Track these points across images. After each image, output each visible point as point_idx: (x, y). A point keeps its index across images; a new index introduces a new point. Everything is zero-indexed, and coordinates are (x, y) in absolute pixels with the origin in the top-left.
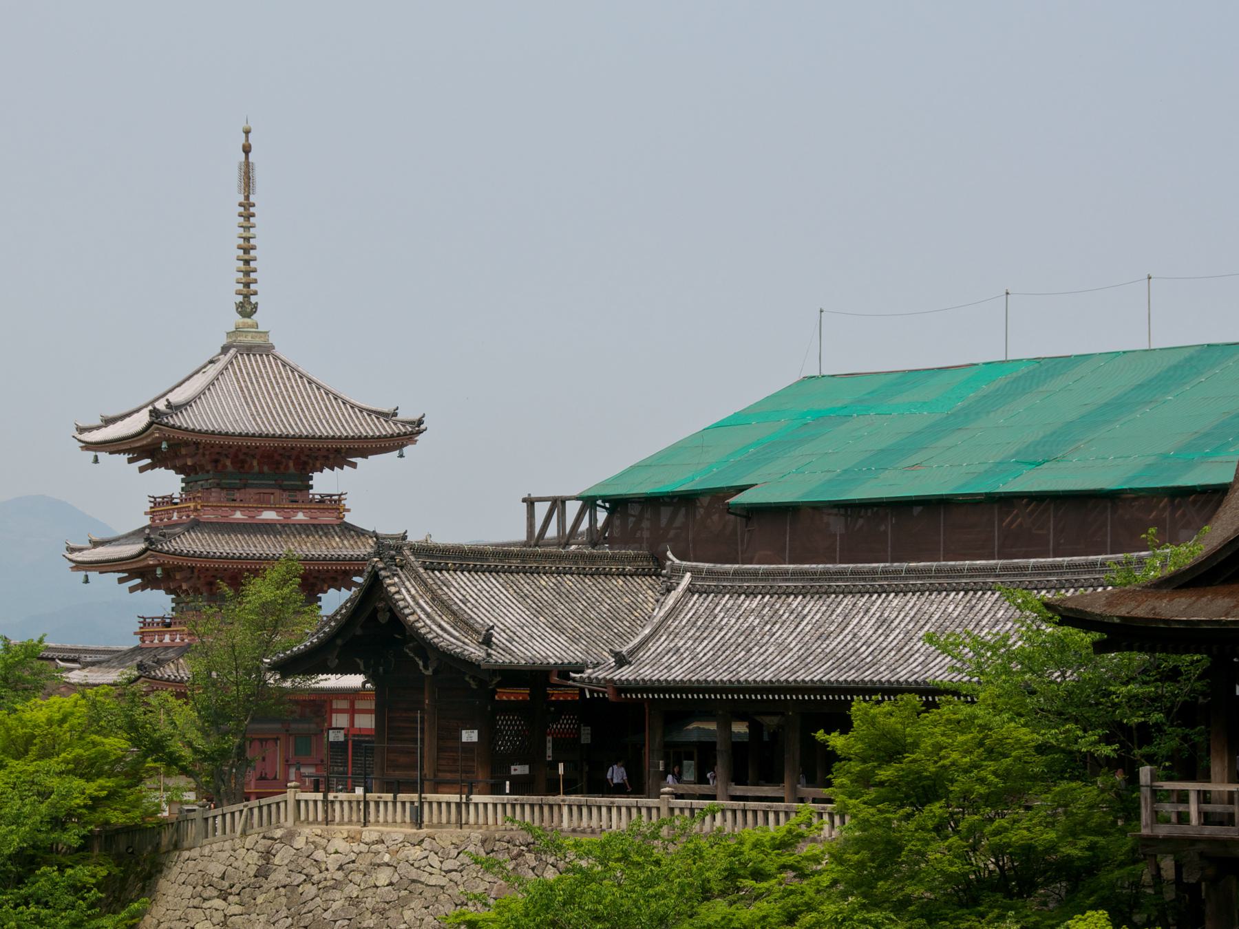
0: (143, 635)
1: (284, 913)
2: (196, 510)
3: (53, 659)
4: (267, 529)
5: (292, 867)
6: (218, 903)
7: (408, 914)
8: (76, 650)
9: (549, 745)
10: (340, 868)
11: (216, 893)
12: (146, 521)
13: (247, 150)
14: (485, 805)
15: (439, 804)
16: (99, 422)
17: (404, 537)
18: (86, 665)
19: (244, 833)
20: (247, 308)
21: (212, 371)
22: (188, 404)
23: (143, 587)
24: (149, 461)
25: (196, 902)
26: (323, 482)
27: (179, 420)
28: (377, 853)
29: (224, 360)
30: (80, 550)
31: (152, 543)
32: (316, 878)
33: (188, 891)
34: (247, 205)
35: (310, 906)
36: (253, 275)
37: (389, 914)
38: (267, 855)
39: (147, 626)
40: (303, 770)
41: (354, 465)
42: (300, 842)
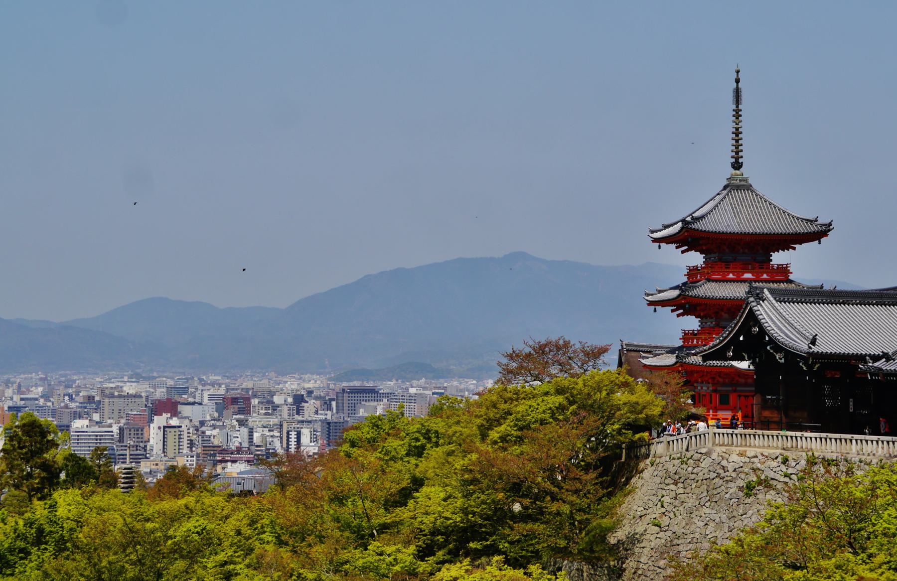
1: (705, 494)
2: (708, 273)
5: (711, 468)
6: (672, 487)
8: (650, 347)
9: (851, 403)
16: (661, 228)
17: (822, 287)
18: (656, 355)
20: (737, 165)
21: (718, 198)
25: (663, 486)
26: (778, 258)
27: (698, 226)
29: (725, 192)
30: (652, 295)
31: (683, 291)
33: (658, 480)
36: (740, 148)
37: (758, 496)
39: (688, 336)
41: (794, 249)
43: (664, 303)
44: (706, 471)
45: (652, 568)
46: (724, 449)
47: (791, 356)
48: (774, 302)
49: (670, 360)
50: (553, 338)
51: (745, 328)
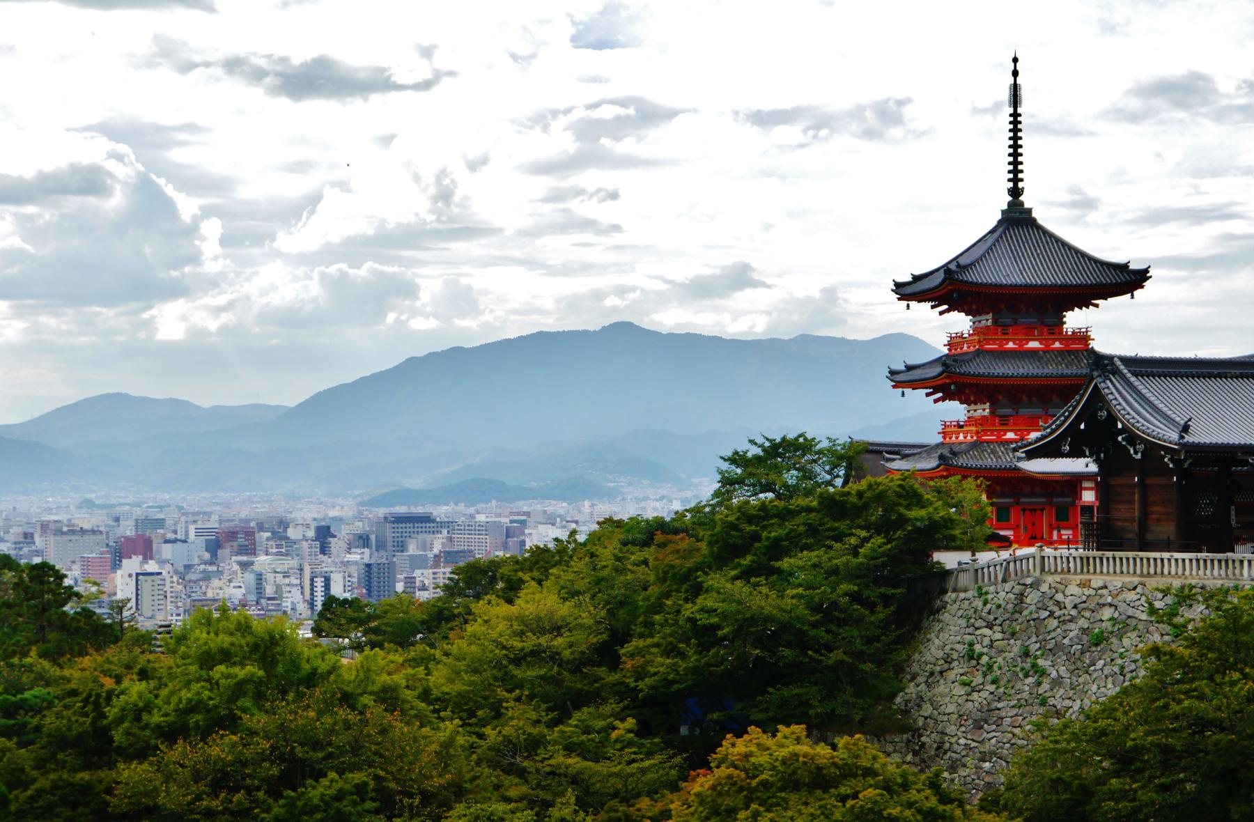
0: (945, 434)
3: (880, 452)
4: (1034, 352)
5: (1040, 605)
6: (986, 631)
7: (1126, 642)
9: (1233, 512)
10: (1075, 607)
11: (985, 624)
12: (945, 350)
13: (1015, 73)
14: (1184, 560)
15: (1148, 559)
16: (909, 279)
18: (905, 457)
19: (1004, 581)
22: (972, 264)
23: (943, 399)
24: (945, 307)
25: (971, 630)
26: (1074, 319)
28: (1101, 596)
32: (1057, 614)
34: (1015, 115)
35: (1053, 635)
38: (1021, 597)
39: (947, 429)
40: (1063, 532)
41: (1097, 306)
42: (1044, 588)
43: (915, 384)
44: (1033, 608)
45: (962, 741)
46: (1058, 578)
47: (1152, 449)
48: (1129, 375)
49: (930, 463)
50: (791, 436)
51: (1088, 413)
